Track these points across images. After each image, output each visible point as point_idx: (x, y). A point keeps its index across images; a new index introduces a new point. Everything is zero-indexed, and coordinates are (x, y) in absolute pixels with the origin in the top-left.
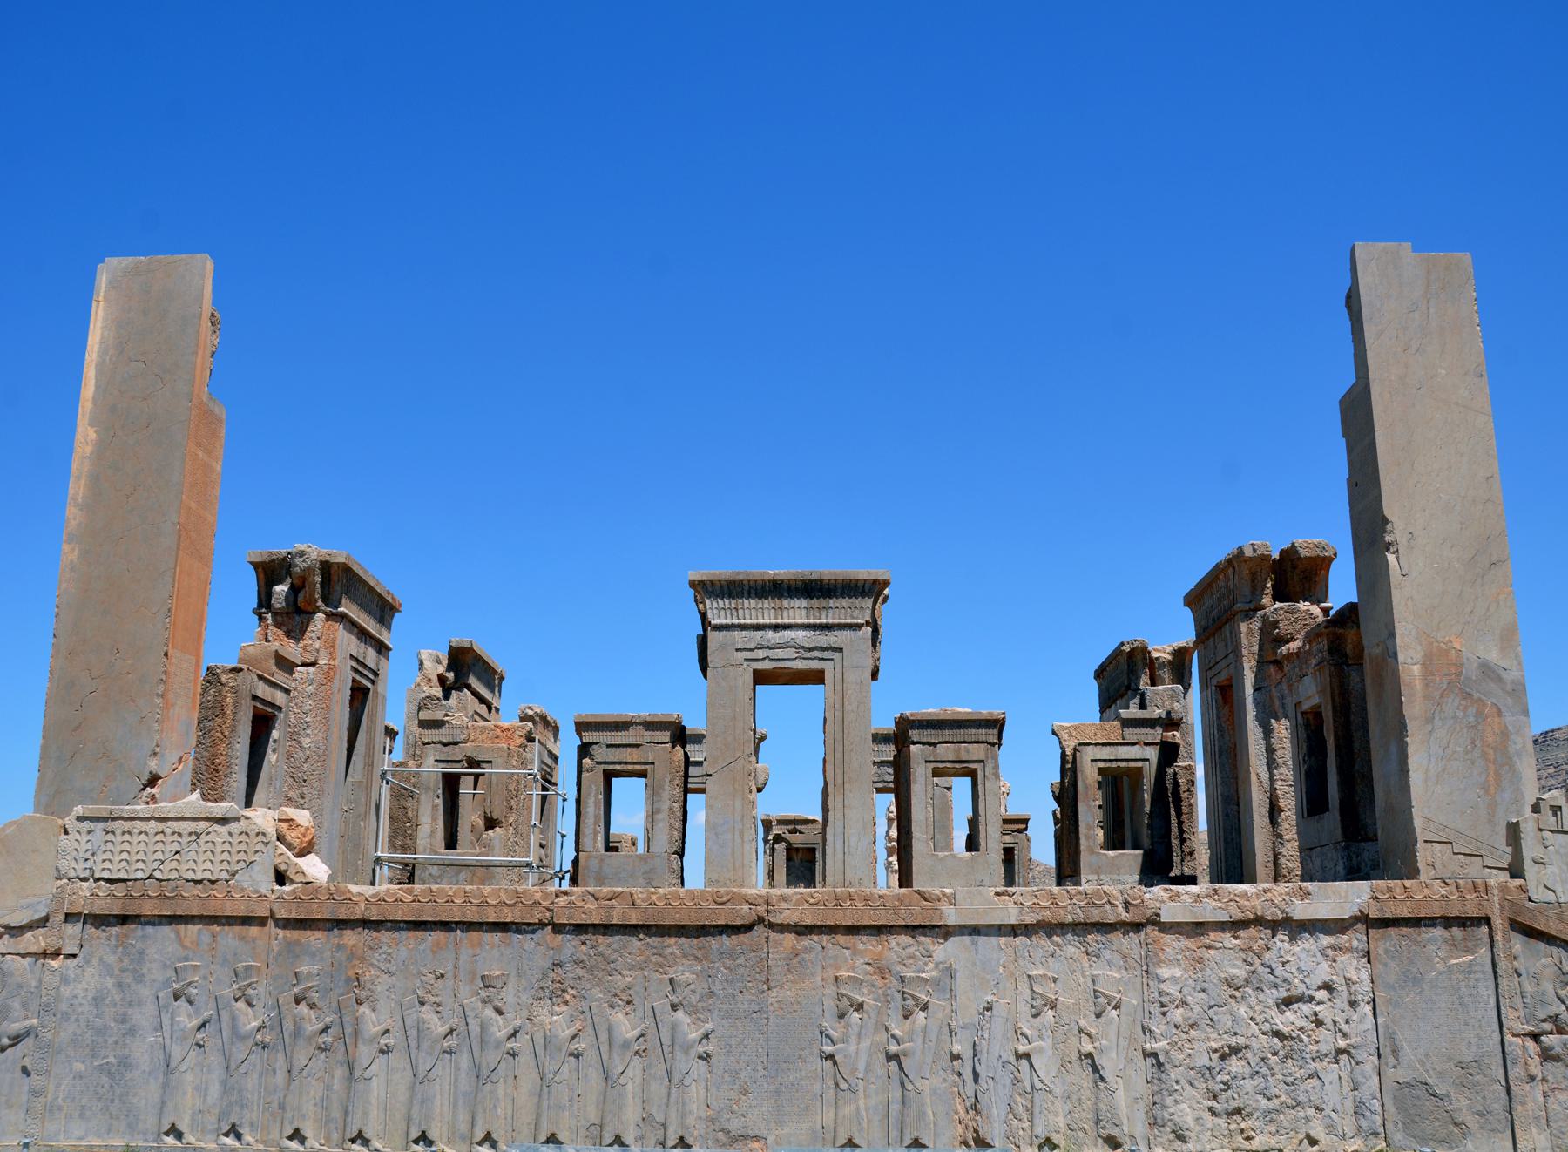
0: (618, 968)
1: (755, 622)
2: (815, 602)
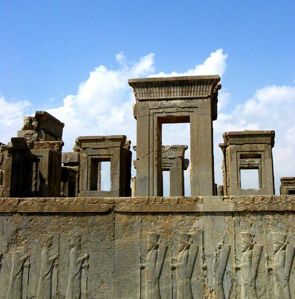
0: (47, 230)
1: (157, 98)
2: (185, 89)
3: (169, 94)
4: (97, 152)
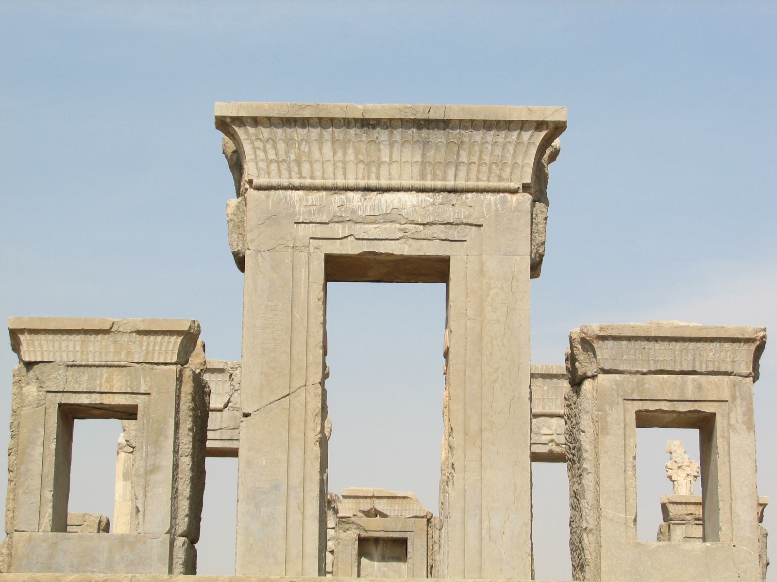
1: (329, 183)
3: (374, 169)
4: (83, 380)
